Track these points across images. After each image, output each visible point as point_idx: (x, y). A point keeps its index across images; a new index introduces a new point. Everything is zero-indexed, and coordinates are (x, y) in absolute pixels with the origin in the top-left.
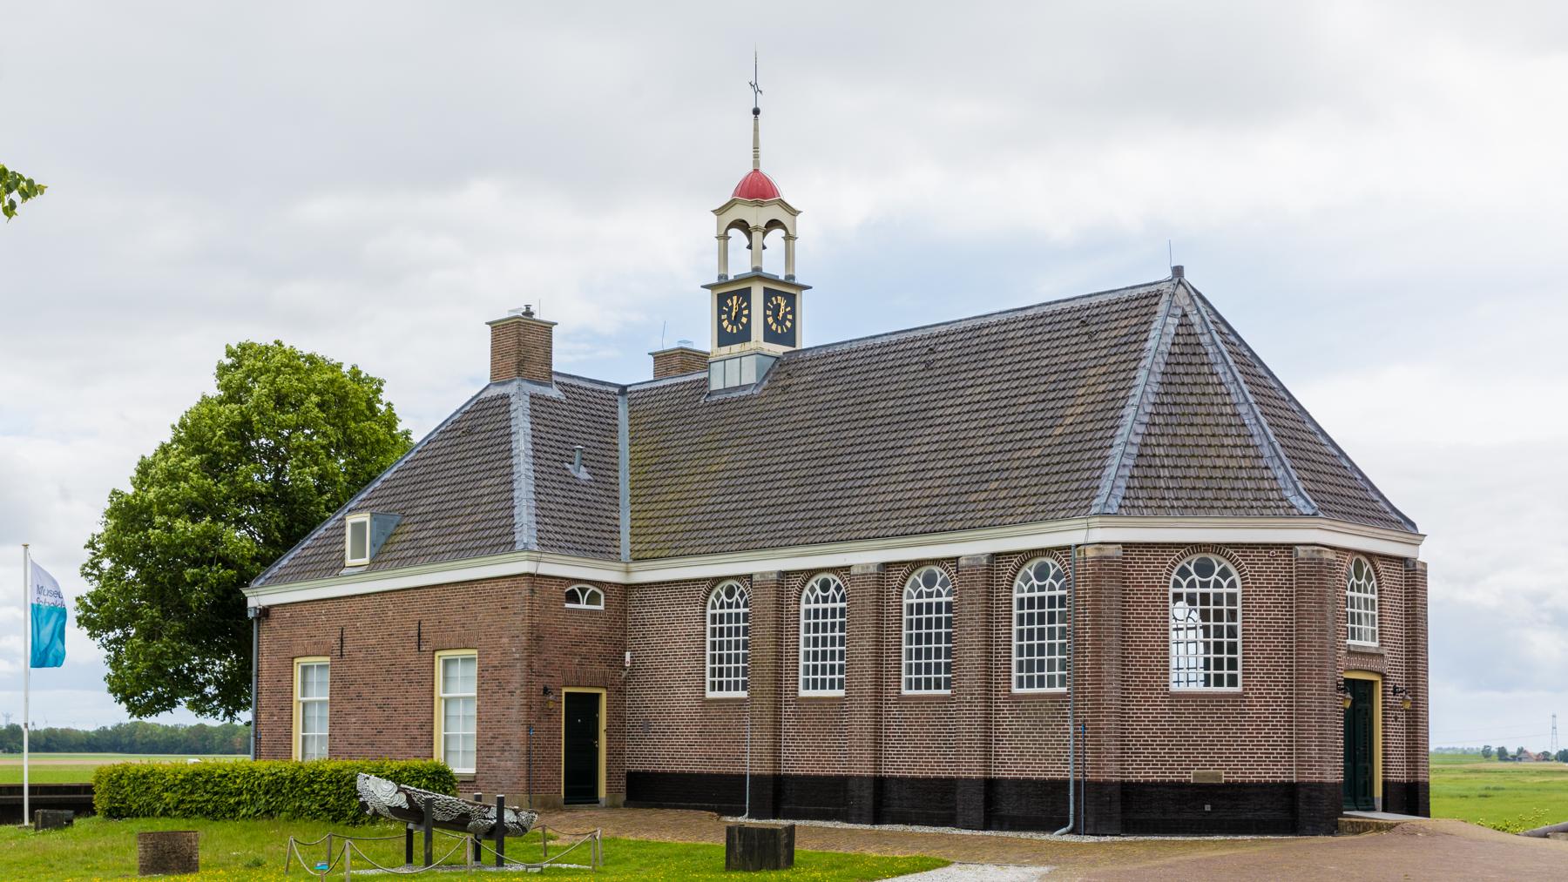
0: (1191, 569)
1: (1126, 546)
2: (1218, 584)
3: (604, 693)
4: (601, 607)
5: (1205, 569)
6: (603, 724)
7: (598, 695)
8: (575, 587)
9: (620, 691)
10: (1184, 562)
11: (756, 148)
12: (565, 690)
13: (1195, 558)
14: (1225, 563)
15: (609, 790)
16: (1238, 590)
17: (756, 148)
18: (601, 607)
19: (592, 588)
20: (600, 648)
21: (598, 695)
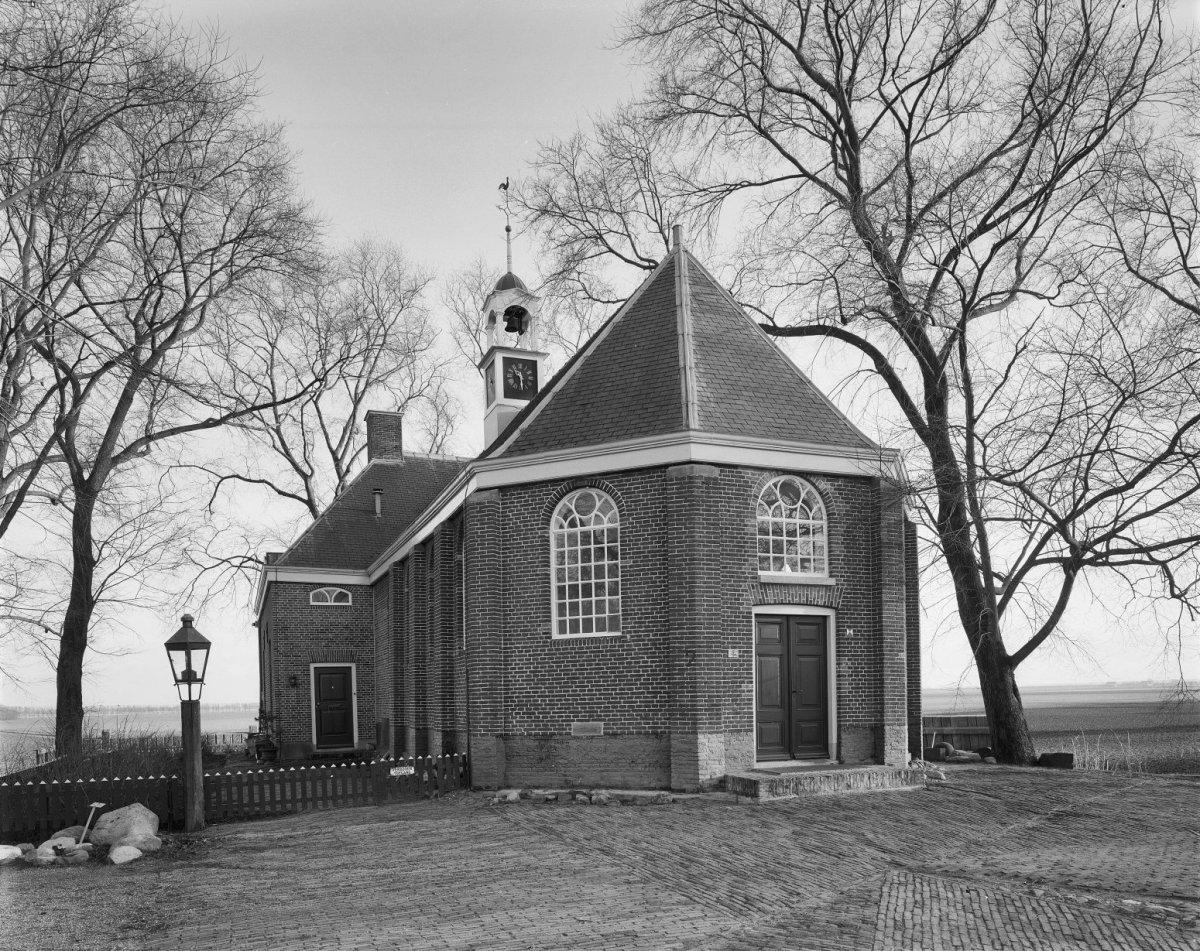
0: (573, 508)
1: (503, 489)
2: (598, 520)
3: (353, 666)
4: (350, 603)
5: (585, 506)
6: (354, 689)
7: (350, 668)
8: (322, 590)
9: (367, 664)
10: (565, 500)
11: (509, 257)
12: (312, 666)
13: (577, 493)
14: (606, 496)
15: (360, 738)
16: (617, 525)
17: (509, 257)
18: (350, 603)
19: (339, 590)
20: (346, 634)
21: (350, 668)
